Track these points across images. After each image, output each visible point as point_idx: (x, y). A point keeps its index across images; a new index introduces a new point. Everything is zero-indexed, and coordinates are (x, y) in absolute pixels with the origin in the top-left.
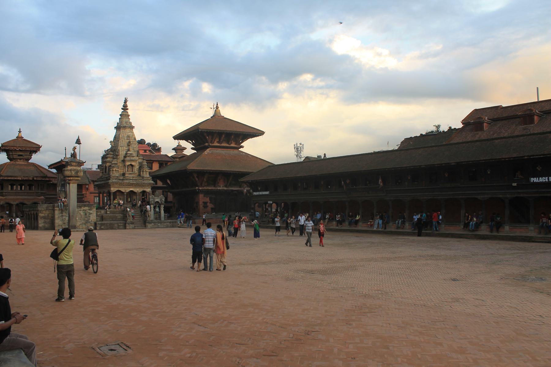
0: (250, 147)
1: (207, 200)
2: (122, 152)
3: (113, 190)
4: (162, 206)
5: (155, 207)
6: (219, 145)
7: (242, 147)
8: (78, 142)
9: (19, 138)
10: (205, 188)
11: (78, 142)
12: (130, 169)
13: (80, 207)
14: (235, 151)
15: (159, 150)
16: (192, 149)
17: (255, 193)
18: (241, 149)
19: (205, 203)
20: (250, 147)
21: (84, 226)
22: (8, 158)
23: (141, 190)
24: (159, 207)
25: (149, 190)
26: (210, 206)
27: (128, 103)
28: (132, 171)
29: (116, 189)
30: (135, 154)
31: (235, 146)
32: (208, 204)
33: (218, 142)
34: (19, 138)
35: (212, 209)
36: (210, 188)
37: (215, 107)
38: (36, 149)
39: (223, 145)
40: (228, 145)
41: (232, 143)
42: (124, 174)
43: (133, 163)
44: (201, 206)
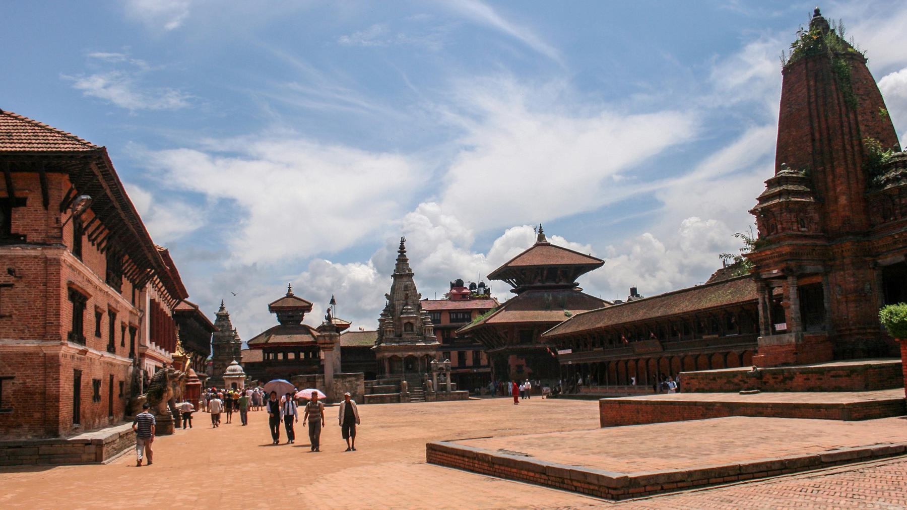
0: (585, 283)
1: (523, 362)
4: (449, 373)
5: (439, 375)
6: (539, 284)
8: (333, 302)
9: (290, 296)
10: (518, 346)
11: (333, 302)
12: (408, 328)
13: (344, 377)
14: (567, 293)
15: (487, 291)
16: (512, 291)
17: (560, 352)
19: (519, 367)
20: (585, 283)
22: (279, 320)
23: (424, 353)
24: (445, 375)
25: (433, 353)
26: (527, 370)
28: (412, 330)
29: (391, 354)
32: (524, 368)
33: (539, 281)
34: (290, 296)
36: (524, 347)
38: (308, 308)
39: (548, 284)
40: (553, 284)
42: (401, 335)
43: (412, 321)
44: (513, 369)
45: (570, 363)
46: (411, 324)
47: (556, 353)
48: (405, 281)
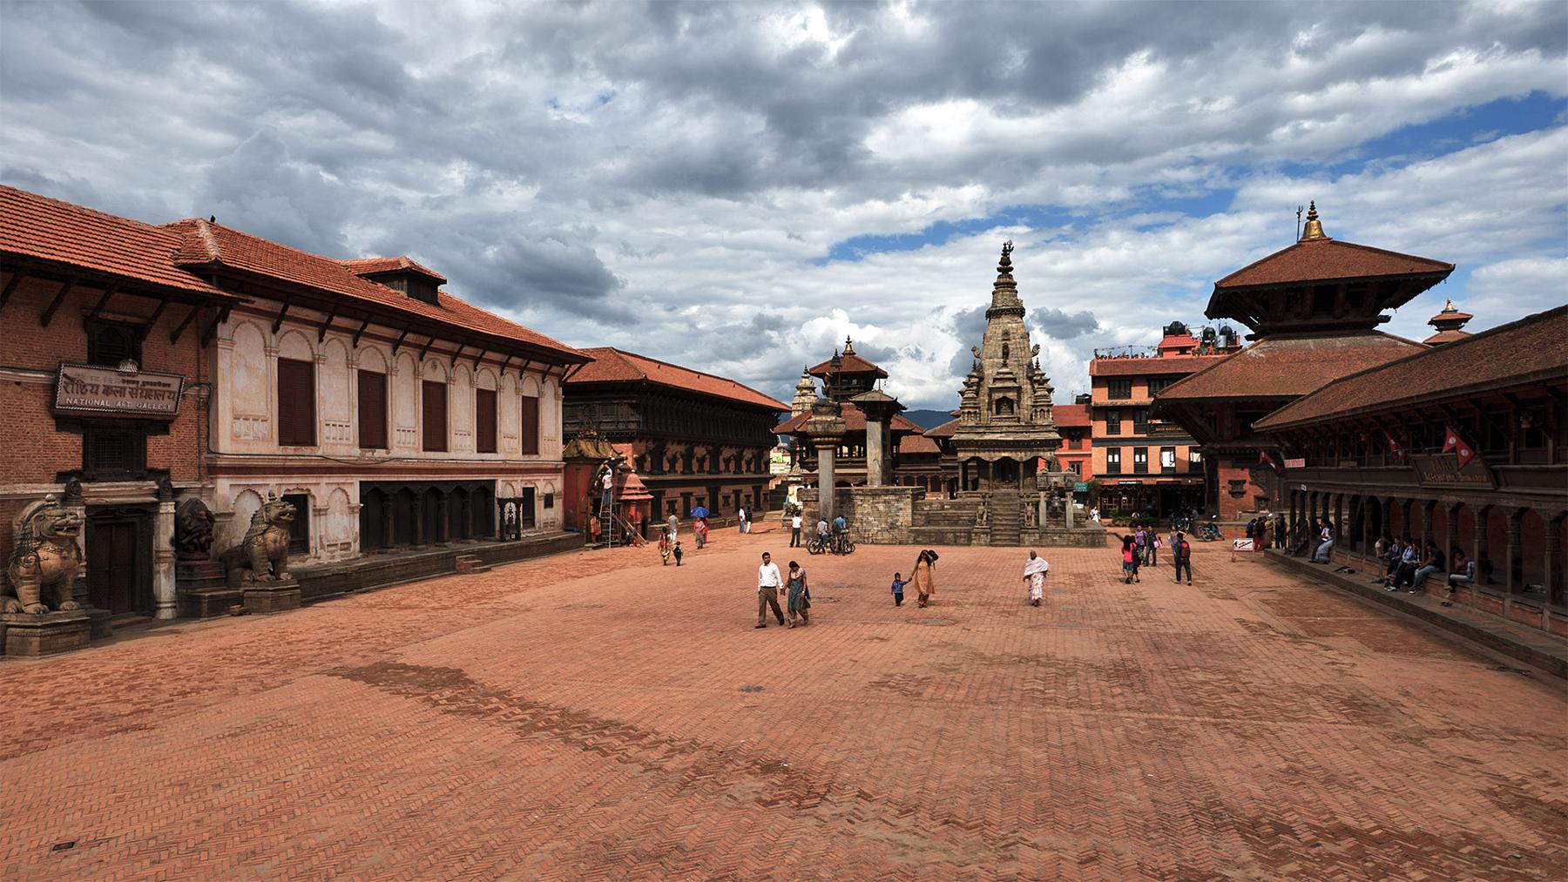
2: (989, 372)
3: (963, 456)
6: (1297, 322)
7: (1387, 319)
10: (1235, 445)
16: (1248, 338)
18: (1381, 327)
21: (886, 535)
27: (1012, 256)
30: (1021, 375)
31: (1360, 319)
32: (1246, 486)
35: (1258, 498)
37: (1305, 214)
41: (1346, 312)
43: (1012, 395)
45: (1304, 488)
46: (1010, 402)
47: (1280, 464)
48: (1007, 323)
